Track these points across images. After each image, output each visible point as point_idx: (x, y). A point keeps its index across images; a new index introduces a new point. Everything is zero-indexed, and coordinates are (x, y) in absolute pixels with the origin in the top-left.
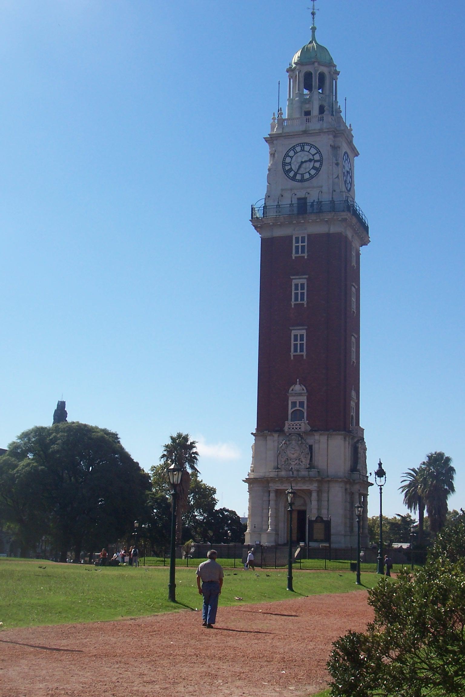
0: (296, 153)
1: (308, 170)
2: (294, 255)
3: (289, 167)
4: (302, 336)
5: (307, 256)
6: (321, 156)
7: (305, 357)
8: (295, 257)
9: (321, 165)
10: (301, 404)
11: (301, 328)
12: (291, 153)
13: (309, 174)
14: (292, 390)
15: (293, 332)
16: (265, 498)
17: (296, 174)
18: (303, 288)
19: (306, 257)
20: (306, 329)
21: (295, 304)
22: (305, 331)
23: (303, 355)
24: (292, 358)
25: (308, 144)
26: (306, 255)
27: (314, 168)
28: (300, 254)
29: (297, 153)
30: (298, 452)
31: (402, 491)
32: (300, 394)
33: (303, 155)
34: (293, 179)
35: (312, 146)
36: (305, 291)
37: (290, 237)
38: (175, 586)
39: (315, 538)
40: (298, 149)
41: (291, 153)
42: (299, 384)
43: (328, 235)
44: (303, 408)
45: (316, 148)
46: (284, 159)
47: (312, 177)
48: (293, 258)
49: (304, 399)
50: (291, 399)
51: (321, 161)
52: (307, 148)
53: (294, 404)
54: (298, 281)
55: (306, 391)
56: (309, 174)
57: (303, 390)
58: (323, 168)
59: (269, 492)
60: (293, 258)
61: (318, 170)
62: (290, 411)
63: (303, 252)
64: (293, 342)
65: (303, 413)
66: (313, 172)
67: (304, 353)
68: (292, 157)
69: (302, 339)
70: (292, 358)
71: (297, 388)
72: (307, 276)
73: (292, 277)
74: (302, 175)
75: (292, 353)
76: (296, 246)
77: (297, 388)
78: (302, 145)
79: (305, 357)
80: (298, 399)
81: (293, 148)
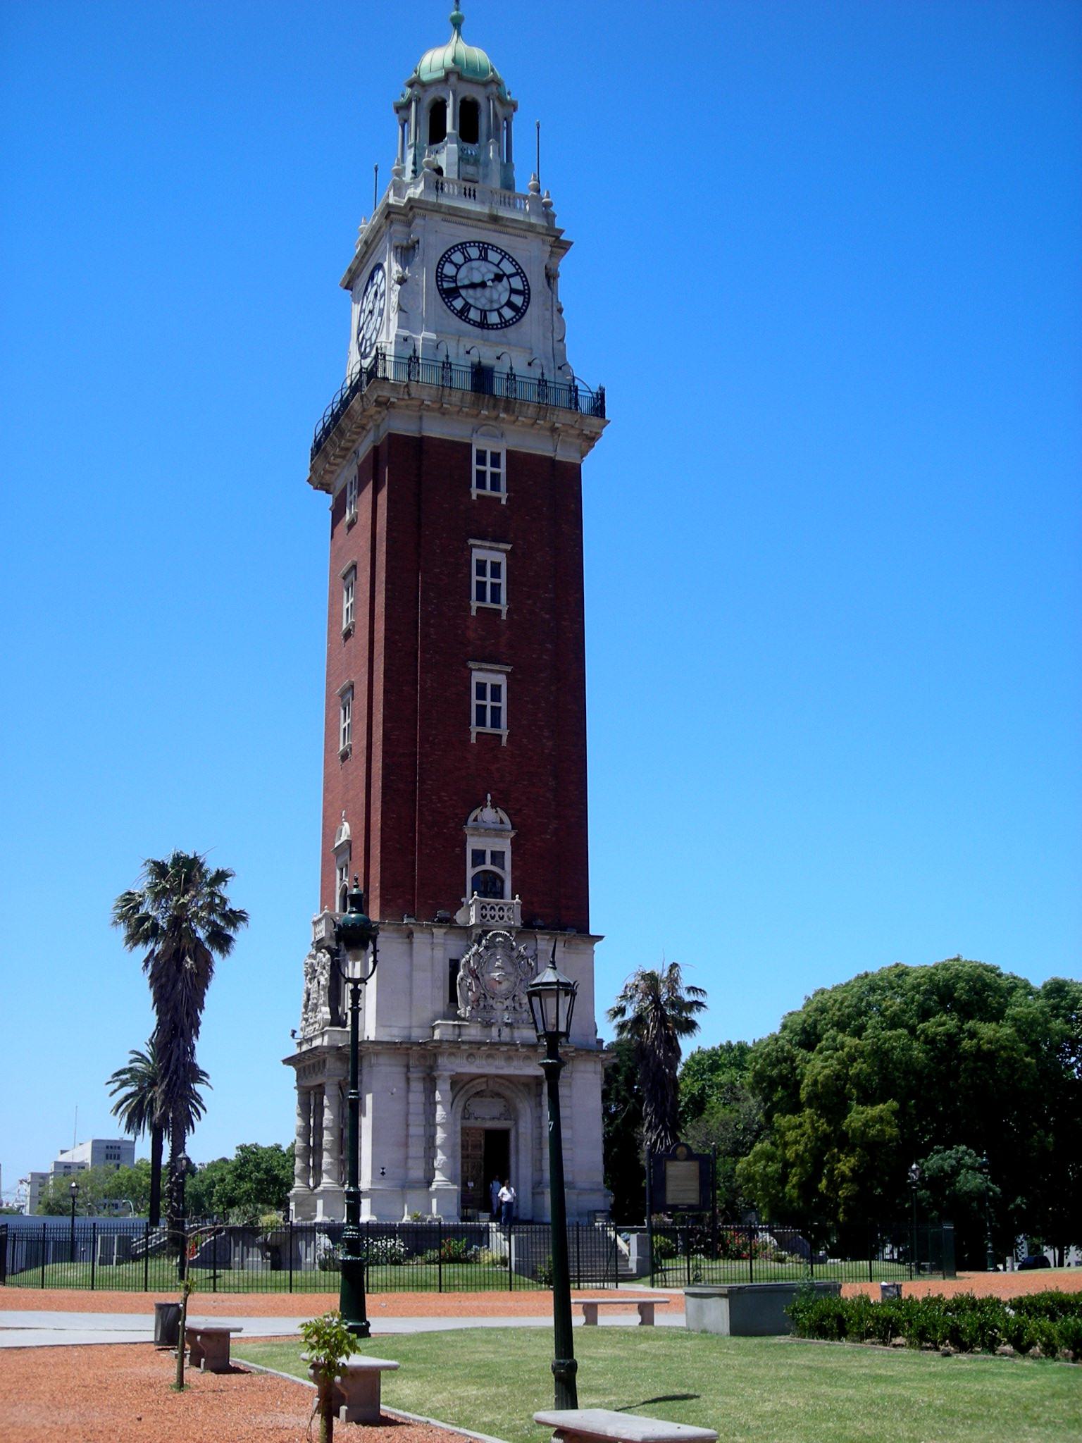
0: (468, 259)
1: (496, 306)
2: (475, 492)
3: (453, 285)
4: (496, 689)
5: (508, 500)
6: (525, 281)
7: (504, 739)
8: (478, 496)
9: (527, 302)
10: (497, 857)
11: (497, 667)
12: (458, 258)
13: (500, 315)
14: (476, 820)
15: (474, 673)
16: (417, 1097)
17: (467, 307)
18: (496, 572)
19: (504, 502)
20: (508, 674)
21: (479, 608)
22: (504, 677)
23: (500, 736)
24: (473, 741)
25: (496, 249)
26: (503, 496)
27: (509, 304)
28: (488, 492)
29: (470, 260)
30: (512, 979)
31: (112, 1094)
32: (498, 833)
33: (484, 270)
34: (462, 314)
35: (505, 255)
36: (503, 581)
37: (469, 446)
38: (573, 1368)
39: (670, 1202)
40: (474, 252)
41: (458, 258)
42: (493, 806)
43: (552, 462)
44: (503, 868)
45: (513, 261)
46: (440, 266)
47: (505, 324)
48: (474, 497)
49: (505, 846)
50: (473, 843)
51: (525, 293)
52: (494, 256)
53: (479, 856)
54: (486, 553)
55: (510, 827)
56: (500, 315)
57: (502, 822)
58: (532, 311)
59: (430, 1083)
60: (474, 497)
61: (520, 312)
62: (470, 872)
63: (495, 486)
64: (475, 702)
65: (502, 882)
66: (508, 313)
67: (504, 731)
68: (458, 267)
69: (496, 696)
70: (473, 741)
71: (488, 815)
72: (509, 547)
73: (472, 541)
74: (484, 313)
75: (474, 729)
76: (478, 471)
77: (488, 815)
78: (484, 248)
79: (504, 739)
80: (490, 845)
81: (462, 247)
